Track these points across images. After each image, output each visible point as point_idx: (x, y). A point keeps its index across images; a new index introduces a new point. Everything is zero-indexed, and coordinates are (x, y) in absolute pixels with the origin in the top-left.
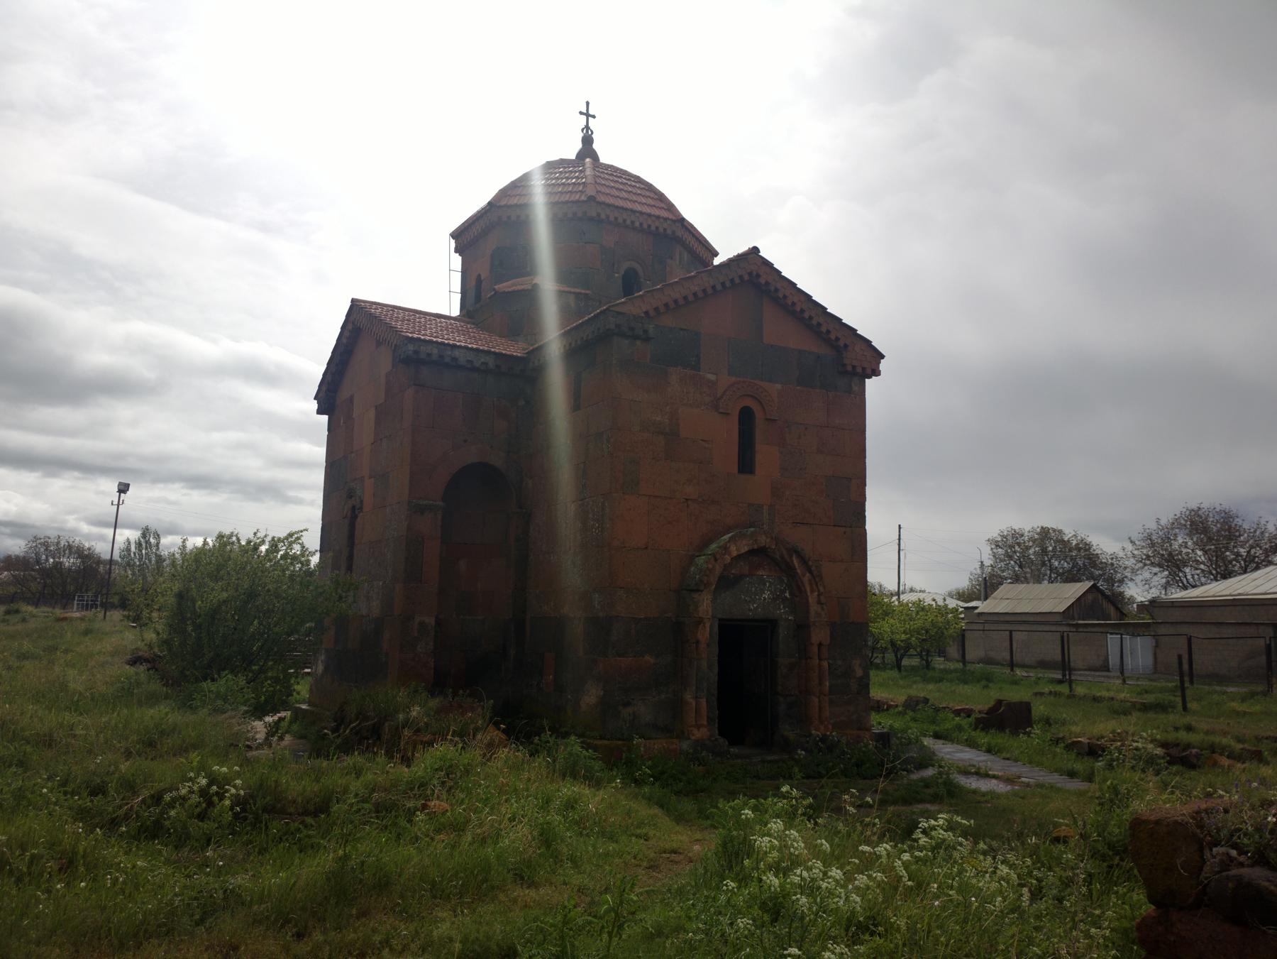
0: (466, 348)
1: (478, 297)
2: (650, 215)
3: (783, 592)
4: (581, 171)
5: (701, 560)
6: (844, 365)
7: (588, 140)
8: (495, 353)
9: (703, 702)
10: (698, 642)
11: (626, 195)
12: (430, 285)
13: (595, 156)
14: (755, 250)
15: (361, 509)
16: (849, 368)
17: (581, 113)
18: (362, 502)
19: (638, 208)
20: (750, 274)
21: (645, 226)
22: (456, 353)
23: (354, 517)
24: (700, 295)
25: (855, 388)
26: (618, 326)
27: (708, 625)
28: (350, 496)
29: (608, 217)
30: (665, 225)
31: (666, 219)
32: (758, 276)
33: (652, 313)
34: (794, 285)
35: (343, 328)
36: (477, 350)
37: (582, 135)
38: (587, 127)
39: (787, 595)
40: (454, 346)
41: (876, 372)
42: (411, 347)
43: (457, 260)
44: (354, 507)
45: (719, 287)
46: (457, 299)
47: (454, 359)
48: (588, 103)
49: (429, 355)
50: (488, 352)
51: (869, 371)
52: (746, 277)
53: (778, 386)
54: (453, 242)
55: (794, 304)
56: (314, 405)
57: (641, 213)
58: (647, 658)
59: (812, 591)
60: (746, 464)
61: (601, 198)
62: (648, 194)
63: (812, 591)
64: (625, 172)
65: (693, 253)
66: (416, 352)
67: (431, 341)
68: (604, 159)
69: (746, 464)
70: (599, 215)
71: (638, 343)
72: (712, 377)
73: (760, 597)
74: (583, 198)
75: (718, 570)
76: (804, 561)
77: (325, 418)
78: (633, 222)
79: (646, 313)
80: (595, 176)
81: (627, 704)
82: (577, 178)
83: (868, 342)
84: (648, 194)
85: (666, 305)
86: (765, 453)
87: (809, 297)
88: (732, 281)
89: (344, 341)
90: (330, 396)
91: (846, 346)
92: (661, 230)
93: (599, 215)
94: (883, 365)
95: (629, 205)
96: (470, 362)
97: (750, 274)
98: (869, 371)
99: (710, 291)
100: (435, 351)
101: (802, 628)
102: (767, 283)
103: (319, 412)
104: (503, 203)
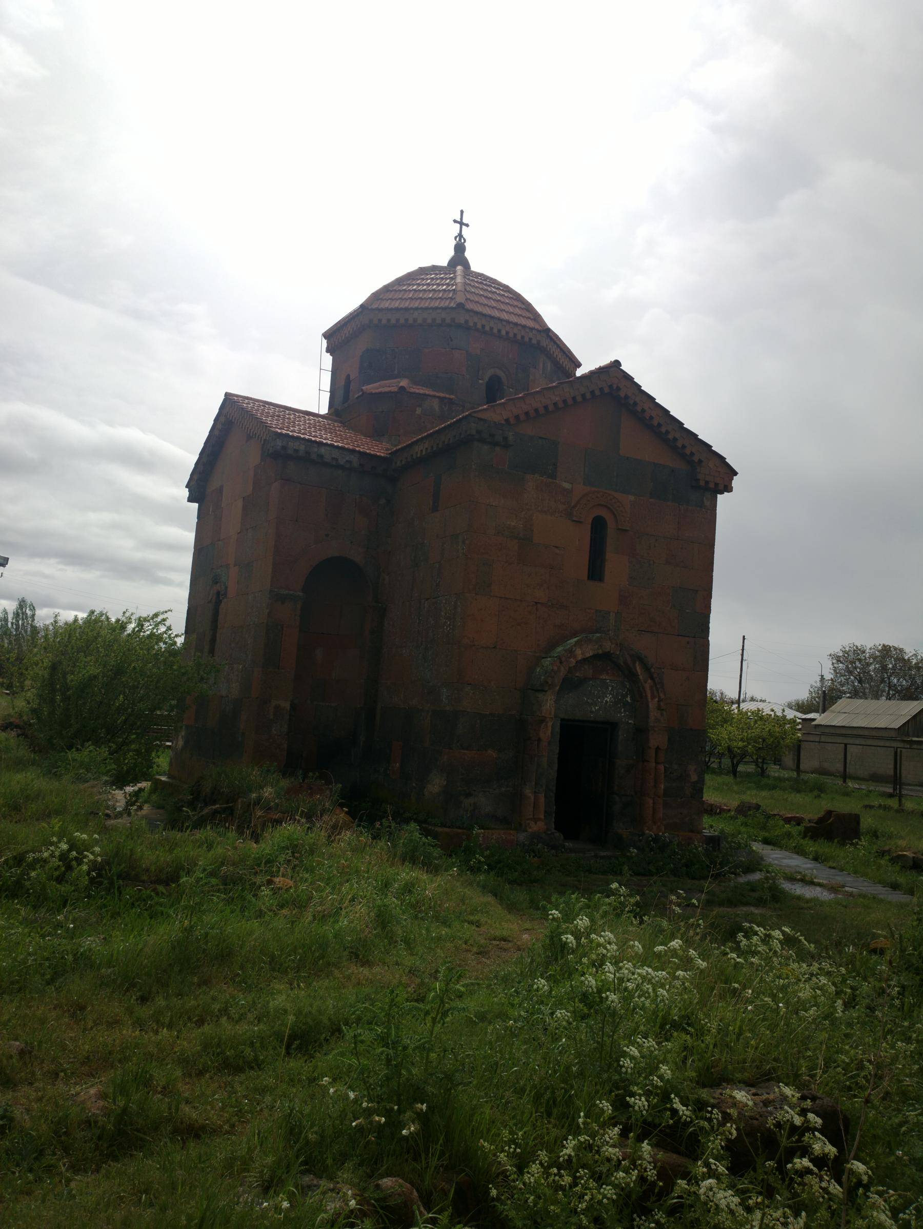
0: (332, 445)
1: (346, 397)
2: (516, 324)
4: (452, 279)
5: (547, 662)
6: (697, 480)
7: (460, 248)
8: (359, 452)
9: (542, 797)
10: (539, 740)
11: (494, 304)
12: (303, 385)
13: (466, 264)
14: (617, 364)
15: (225, 594)
16: (702, 483)
17: (455, 221)
18: (226, 588)
19: (505, 316)
20: (610, 387)
21: (511, 335)
22: (323, 450)
23: (218, 603)
24: (561, 405)
25: (707, 503)
26: (479, 432)
27: (550, 724)
28: (216, 581)
29: (475, 324)
30: (531, 335)
31: (532, 329)
32: (618, 389)
33: (512, 421)
34: (653, 399)
35: (216, 420)
36: (342, 448)
37: (454, 242)
38: (460, 235)
39: (629, 699)
40: (321, 444)
41: (728, 489)
42: (279, 443)
43: (328, 359)
44: (218, 593)
45: (579, 399)
46: (326, 397)
47: (321, 456)
48: (462, 212)
49: (296, 451)
50: (353, 451)
51: (721, 487)
52: (606, 390)
53: (632, 498)
54: (325, 342)
55: (651, 418)
56: (186, 493)
57: (508, 322)
58: (490, 752)
59: (653, 697)
60: (596, 572)
61: (470, 306)
62: (516, 303)
63: (653, 697)
64: (494, 281)
65: (555, 363)
66: (284, 448)
67: (299, 438)
68: (474, 267)
69: (596, 572)
70: (467, 322)
71: (498, 449)
72: (566, 485)
73: (603, 700)
74: (453, 305)
75: (563, 672)
76: (647, 668)
77: (195, 506)
78: (499, 331)
79: (507, 420)
80: (465, 284)
81: (468, 795)
82: (448, 285)
83: (722, 459)
84: (516, 303)
85: (527, 413)
86: (616, 565)
87: (666, 412)
88: (592, 392)
89: (216, 433)
90: (201, 484)
91: (700, 461)
92: (527, 339)
93: (467, 322)
95: (496, 314)
96: (336, 460)
97: (610, 387)
99: (570, 402)
100: (302, 448)
101: (641, 732)
102: (627, 397)
103: (190, 500)
104: (374, 306)
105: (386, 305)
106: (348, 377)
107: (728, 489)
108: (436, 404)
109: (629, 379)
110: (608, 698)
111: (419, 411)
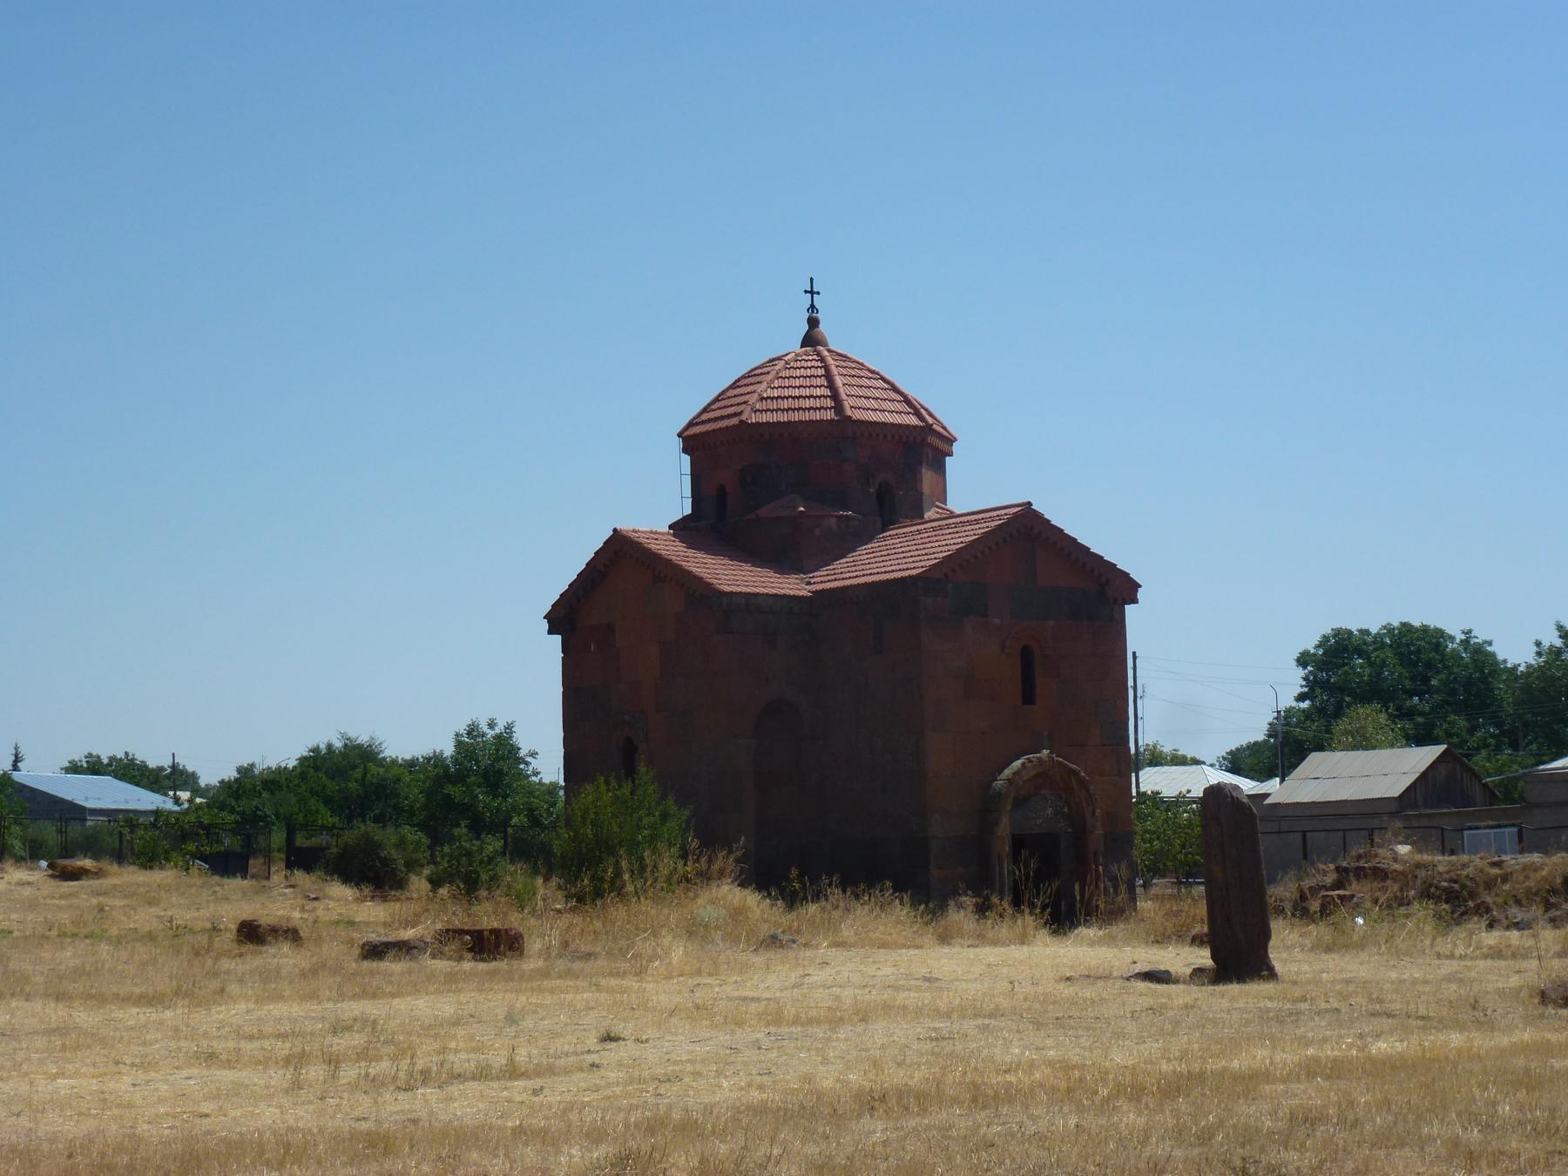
7: (813, 322)
38: (812, 306)
41: (1134, 601)
43: (686, 459)
53: (1052, 623)
56: (545, 625)
60: (1028, 698)
69: (1028, 698)
72: (997, 621)
77: (558, 638)
94: (1141, 594)
103: (550, 632)
106: (721, 489)
107: (1134, 601)
108: (833, 521)
110: (1049, 811)
111: (817, 532)
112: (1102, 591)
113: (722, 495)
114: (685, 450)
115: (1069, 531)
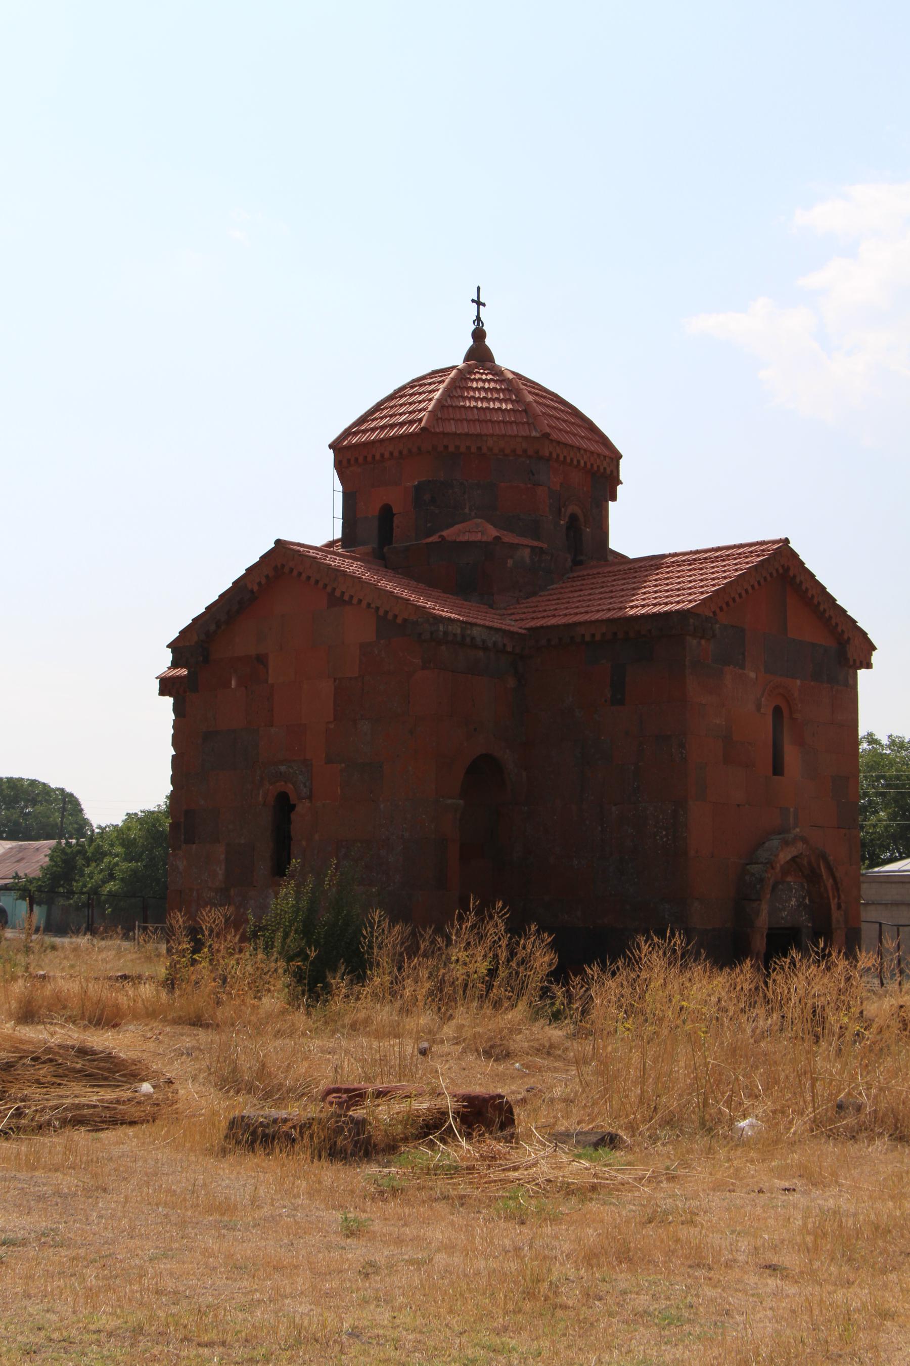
3: (804, 898)
7: (479, 335)
22: (475, 632)
25: (851, 682)
34: (813, 576)
37: (474, 327)
38: (478, 319)
39: (807, 901)
41: (869, 666)
48: (479, 288)
49: (455, 635)
51: (858, 664)
53: (798, 682)
59: (834, 897)
61: (555, 435)
63: (834, 897)
76: (830, 869)
83: (864, 634)
87: (823, 588)
94: (875, 657)
97: (783, 566)
98: (861, 662)
105: (452, 428)
107: (869, 666)
108: (526, 553)
109: (795, 555)
111: (510, 562)
112: (847, 647)
113: (387, 514)
114: (340, 466)
115: (821, 577)
